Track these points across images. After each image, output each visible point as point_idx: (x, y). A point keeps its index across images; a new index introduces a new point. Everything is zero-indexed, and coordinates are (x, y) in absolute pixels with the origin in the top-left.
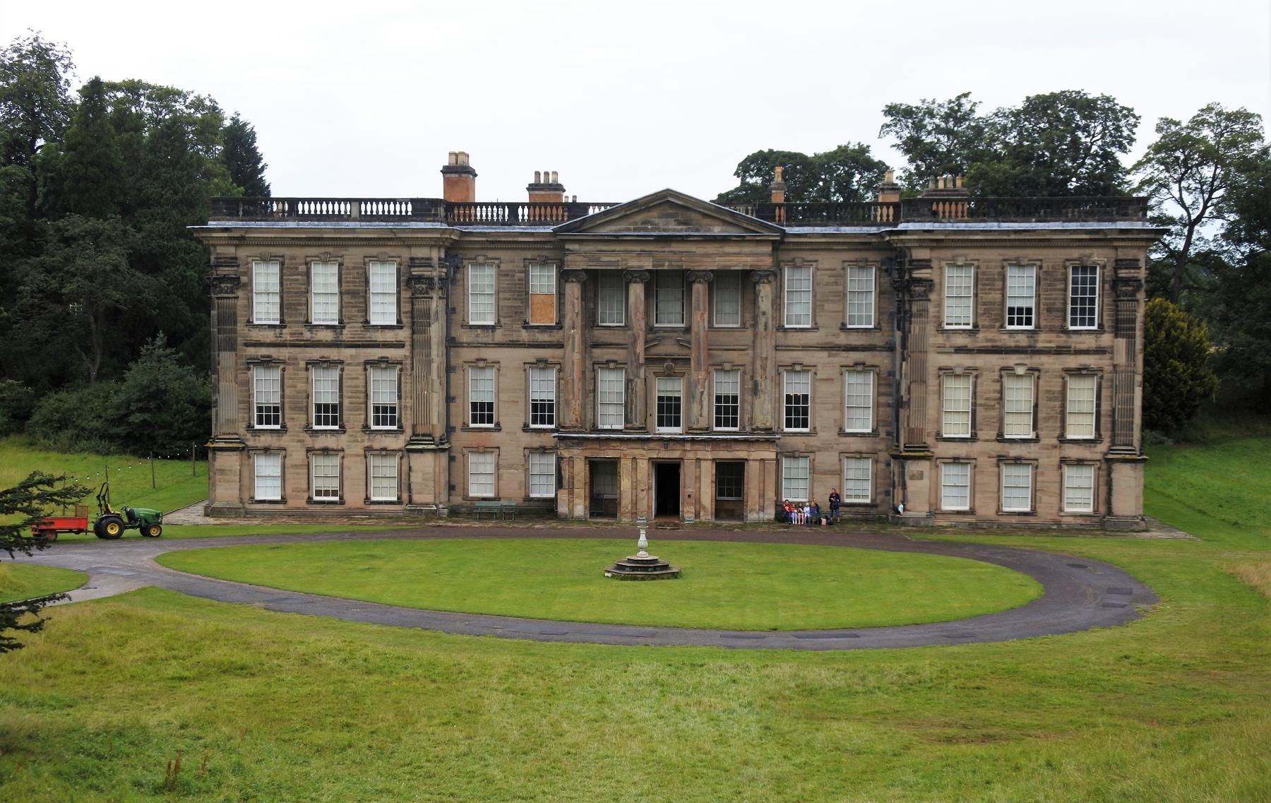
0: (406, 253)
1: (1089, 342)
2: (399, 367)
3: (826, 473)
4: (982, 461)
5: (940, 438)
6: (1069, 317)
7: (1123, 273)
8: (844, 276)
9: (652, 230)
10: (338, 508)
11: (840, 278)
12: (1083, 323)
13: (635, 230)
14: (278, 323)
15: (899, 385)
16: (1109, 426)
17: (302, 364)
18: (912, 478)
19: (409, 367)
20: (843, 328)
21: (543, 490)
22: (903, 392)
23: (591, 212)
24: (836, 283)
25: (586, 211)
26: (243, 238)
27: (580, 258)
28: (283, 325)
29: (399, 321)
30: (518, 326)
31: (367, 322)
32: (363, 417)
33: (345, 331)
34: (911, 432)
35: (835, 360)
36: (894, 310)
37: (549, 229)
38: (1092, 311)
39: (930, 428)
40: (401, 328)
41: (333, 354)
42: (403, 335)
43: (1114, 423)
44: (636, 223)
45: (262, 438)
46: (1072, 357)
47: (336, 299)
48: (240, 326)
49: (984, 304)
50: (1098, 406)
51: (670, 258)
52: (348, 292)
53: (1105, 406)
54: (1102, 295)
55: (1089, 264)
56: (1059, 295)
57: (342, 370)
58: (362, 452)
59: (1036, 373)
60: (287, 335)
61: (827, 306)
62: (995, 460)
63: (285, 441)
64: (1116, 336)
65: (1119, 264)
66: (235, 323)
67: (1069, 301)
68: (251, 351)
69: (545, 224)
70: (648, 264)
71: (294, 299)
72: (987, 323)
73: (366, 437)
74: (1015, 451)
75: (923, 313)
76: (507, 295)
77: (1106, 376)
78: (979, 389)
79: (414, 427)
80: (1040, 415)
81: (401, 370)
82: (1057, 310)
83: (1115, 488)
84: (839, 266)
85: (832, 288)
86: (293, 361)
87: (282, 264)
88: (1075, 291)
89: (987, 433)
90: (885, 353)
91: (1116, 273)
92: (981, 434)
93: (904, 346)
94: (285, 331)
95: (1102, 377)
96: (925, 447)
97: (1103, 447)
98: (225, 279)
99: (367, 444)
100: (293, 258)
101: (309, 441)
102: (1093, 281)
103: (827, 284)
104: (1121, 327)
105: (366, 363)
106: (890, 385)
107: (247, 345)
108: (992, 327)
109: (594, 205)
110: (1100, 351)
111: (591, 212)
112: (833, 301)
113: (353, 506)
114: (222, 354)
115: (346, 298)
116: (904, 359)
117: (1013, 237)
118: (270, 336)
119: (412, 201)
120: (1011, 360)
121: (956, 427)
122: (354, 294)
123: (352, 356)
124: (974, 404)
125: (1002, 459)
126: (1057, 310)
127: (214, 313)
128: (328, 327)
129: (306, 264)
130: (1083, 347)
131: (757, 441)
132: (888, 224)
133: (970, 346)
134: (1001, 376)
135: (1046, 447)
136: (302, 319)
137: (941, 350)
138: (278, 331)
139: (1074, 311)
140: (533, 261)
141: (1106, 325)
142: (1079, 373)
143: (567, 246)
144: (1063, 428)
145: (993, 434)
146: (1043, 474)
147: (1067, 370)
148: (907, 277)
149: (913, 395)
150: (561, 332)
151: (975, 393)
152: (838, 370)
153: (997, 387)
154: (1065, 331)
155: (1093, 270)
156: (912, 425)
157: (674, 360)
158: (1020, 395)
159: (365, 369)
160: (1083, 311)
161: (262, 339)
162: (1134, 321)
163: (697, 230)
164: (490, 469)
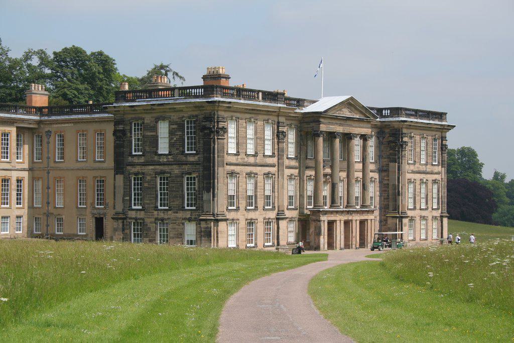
29: (273, 153)
42: (274, 160)
43: (442, 201)
99: (264, 216)
107: (227, 164)
145: (419, 208)
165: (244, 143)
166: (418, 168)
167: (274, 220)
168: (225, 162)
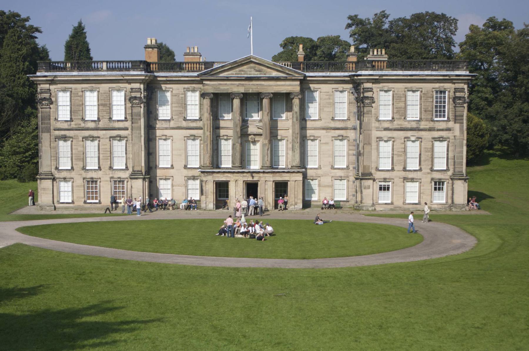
0: (129, 86)
1: (443, 125)
2: (126, 139)
3: (325, 186)
4: (396, 180)
5: (377, 169)
6: (434, 114)
7: (458, 94)
8: (333, 95)
9: (244, 74)
10: (98, 205)
11: (331, 96)
12: (440, 116)
13: (236, 74)
14: (69, 119)
15: (358, 145)
16: (453, 163)
17: (81, 139)
18: (365, 188)
19: (130, 139)
20: (333, 119)
21: (195, 195)
22: (361, 148)
23: (216, 66)
24: (329, 99)
25: (213, 66)
26: (53, 80)
27: (211, 88)
28: (71, 120)
29: (126, 118)
30: (181, 119)
31: (110, 118)
32: (109, 163)
33: (100, 123)
34: (364, 167)
35: (329, 134)
36: (355, 110)
37: (196, 74)
38: (444, 111)
39: (374, 165)
40: (127, 121)
41: (95, 133)
44: (236, 71)
45: (63, 173)
46: (436, 132)
47: (96, 108)
48: (52, 121)
49: (397, 108)
50: (448, 154)
51: (252, 87)
52: (102, 105)
53: (451, 155)
54: (449, 104)
55: (443, 90)
56: (430, 104)
57: (99, 141)
58: (109, 179)
59: (420, 140)
60: (73, 125)
61: (325, 109)
62: (402, 180)
63: (73, 174)
64: (455, 123)
65: (456, 90)
66: (50, 119)
67: (434, 107)
68: (57, 133)
69: (194, 71)
70: (242, 90)
71: (77, 108)
72: (398, 117)
73: (111, 172)
74: (411, 175)
75: (369, 112)
76: (176, 105)
77: (451, 141)
78: (395, 147)
79: (133, 167)
80: (422, 159)
81: (127, 141)
82: (429, 111)
83: (455, 191)
84: (331, 90)
85: (328, 101)
86: (76, 137)
87: (71, 92)
88: (437, 102)
89: (399, 167)
90: (352, 131)
91: (455, 94)
92: (395, 168)
93: (361, 128)
94: (72, 123)
95: (449, 142)
96: (371, 174)
97: (450, 173)
98: (45, 99)
99: (111, 175)
100: (76, 89)
101: (84, 175)
102: (445, 97)
103: (325, 99)
104: (457, 119)
105: (110, 137)
106: (354, 146)
107: (55, 130)
108: (400, 119)
109: (217, 62)
110: (449, 130)
111: (216, 66)
112: (328, 107)
113: (105, 205)
114: (43, 134)
115: (101, 108)
116: (360, 134)
117: (409, 78)
118: (65, 126)
119: (132, 62)
120: (409, 134)
121: (385, 164)
122: (104, 105)
123: (104, 135)
124: (393, 154)
125: (405, 179)
126: (429, 111)
127: (40, 115)
128: (92, 121)
129: (82, 92)
130: (441, 128)
131: (294, 172)
132: (352, 71)
133: (391, 127)
134: (405, 141)
135: (425, 174)
136: (81, 117)
137: (378, 129)
138: (69, 123)
139: (436, 111)
140: (188, 90)
141: (451, 117)
142: (441, 139)
143: (204, 82)
144: (432, 165)
146: (423, 186)
147: (433, 138)
148: (362, 96)
149: (365, 150)
150: (201, 122)
151: (393, 149)
152: (331, 139)
153: (403, 146)
154: (433, 121)
155: (445, 92)
156: (365, 164)
157: (255, 135)
158: (413, 149)
159: (110, 141)
160: (440, 111)
161: (62, 127)
162: (462, 116)
163: (265, 74)
164: (169, 187)
165: (79, 111)
166: (398, 125)
167: (127, 180)
168: (52, 128)
